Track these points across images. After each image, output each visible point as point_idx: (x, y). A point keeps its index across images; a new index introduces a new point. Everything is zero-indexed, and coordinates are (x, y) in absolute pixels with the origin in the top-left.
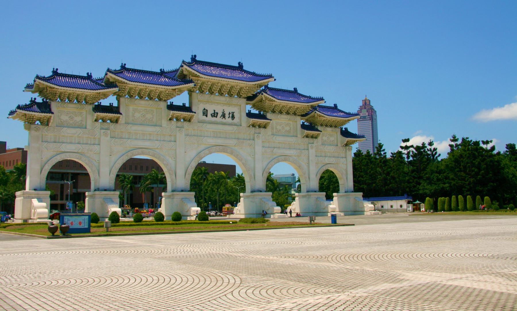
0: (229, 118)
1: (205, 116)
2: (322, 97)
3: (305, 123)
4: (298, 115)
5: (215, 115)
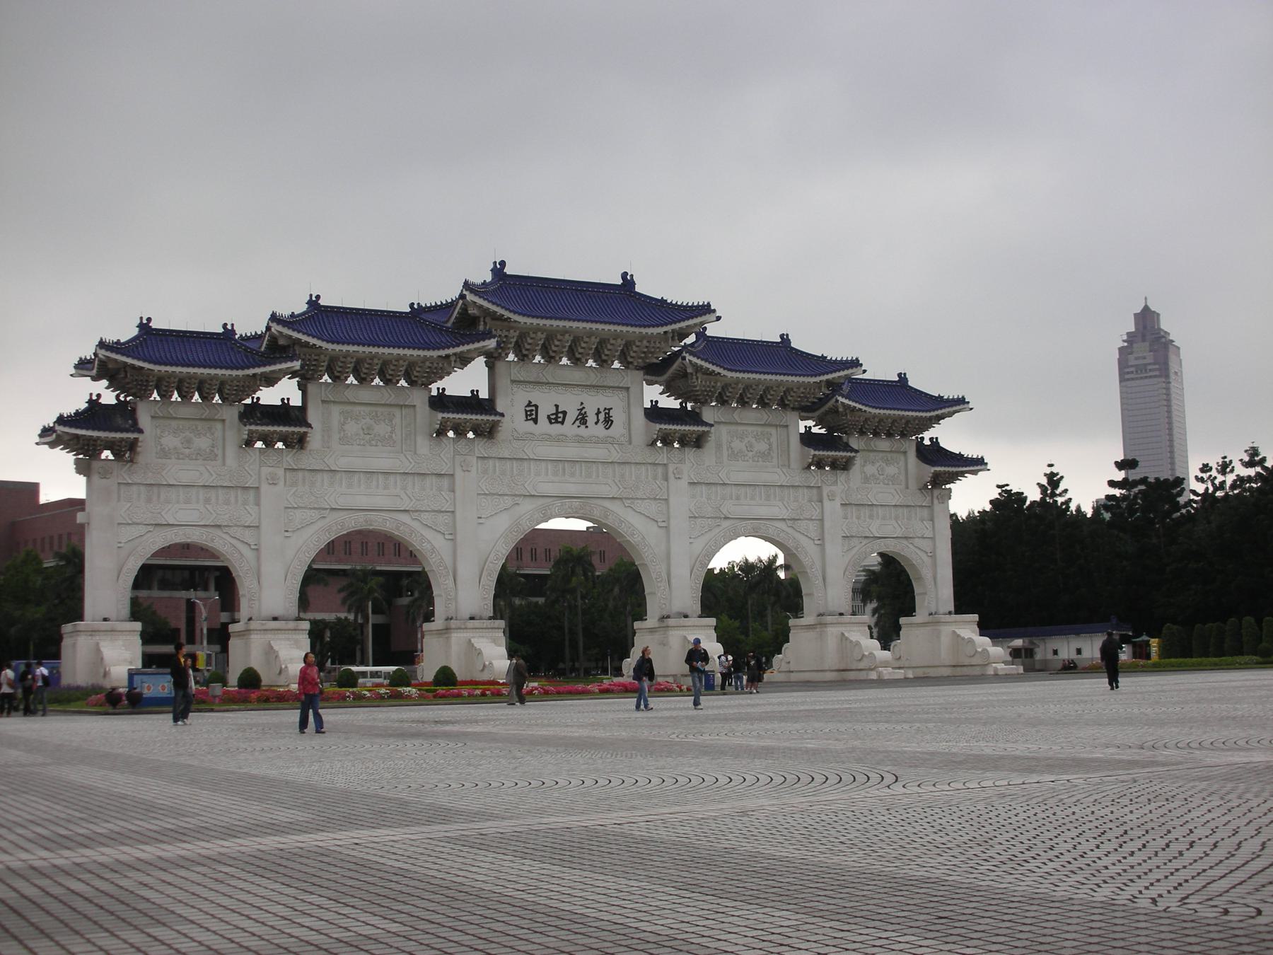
0: (596, 423)
1: (531, 422)
2: (857, 359)
3: (815, 430)
4: (793, 409)
5: (558, 417)
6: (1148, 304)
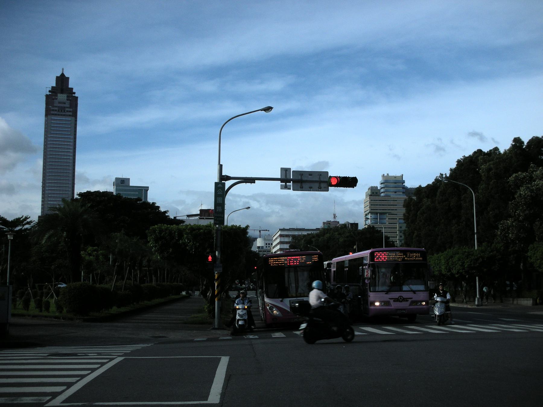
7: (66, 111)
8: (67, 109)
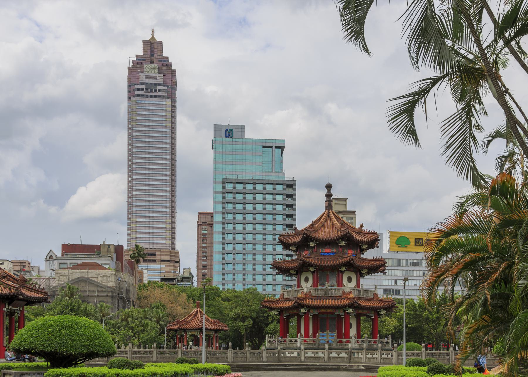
6: (155, 36)
7: (158, 91)
8: (159, 88)
